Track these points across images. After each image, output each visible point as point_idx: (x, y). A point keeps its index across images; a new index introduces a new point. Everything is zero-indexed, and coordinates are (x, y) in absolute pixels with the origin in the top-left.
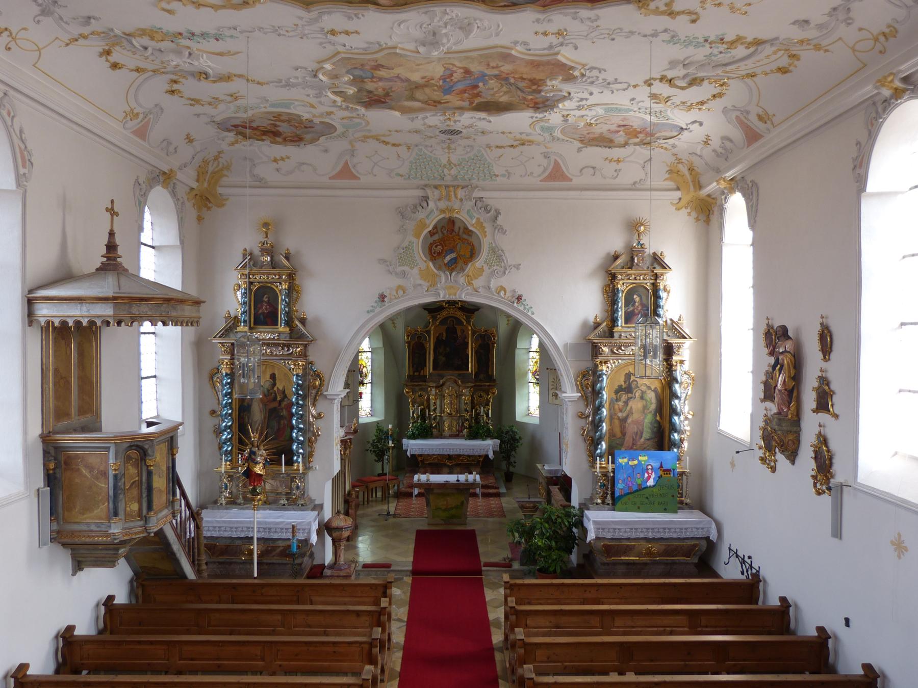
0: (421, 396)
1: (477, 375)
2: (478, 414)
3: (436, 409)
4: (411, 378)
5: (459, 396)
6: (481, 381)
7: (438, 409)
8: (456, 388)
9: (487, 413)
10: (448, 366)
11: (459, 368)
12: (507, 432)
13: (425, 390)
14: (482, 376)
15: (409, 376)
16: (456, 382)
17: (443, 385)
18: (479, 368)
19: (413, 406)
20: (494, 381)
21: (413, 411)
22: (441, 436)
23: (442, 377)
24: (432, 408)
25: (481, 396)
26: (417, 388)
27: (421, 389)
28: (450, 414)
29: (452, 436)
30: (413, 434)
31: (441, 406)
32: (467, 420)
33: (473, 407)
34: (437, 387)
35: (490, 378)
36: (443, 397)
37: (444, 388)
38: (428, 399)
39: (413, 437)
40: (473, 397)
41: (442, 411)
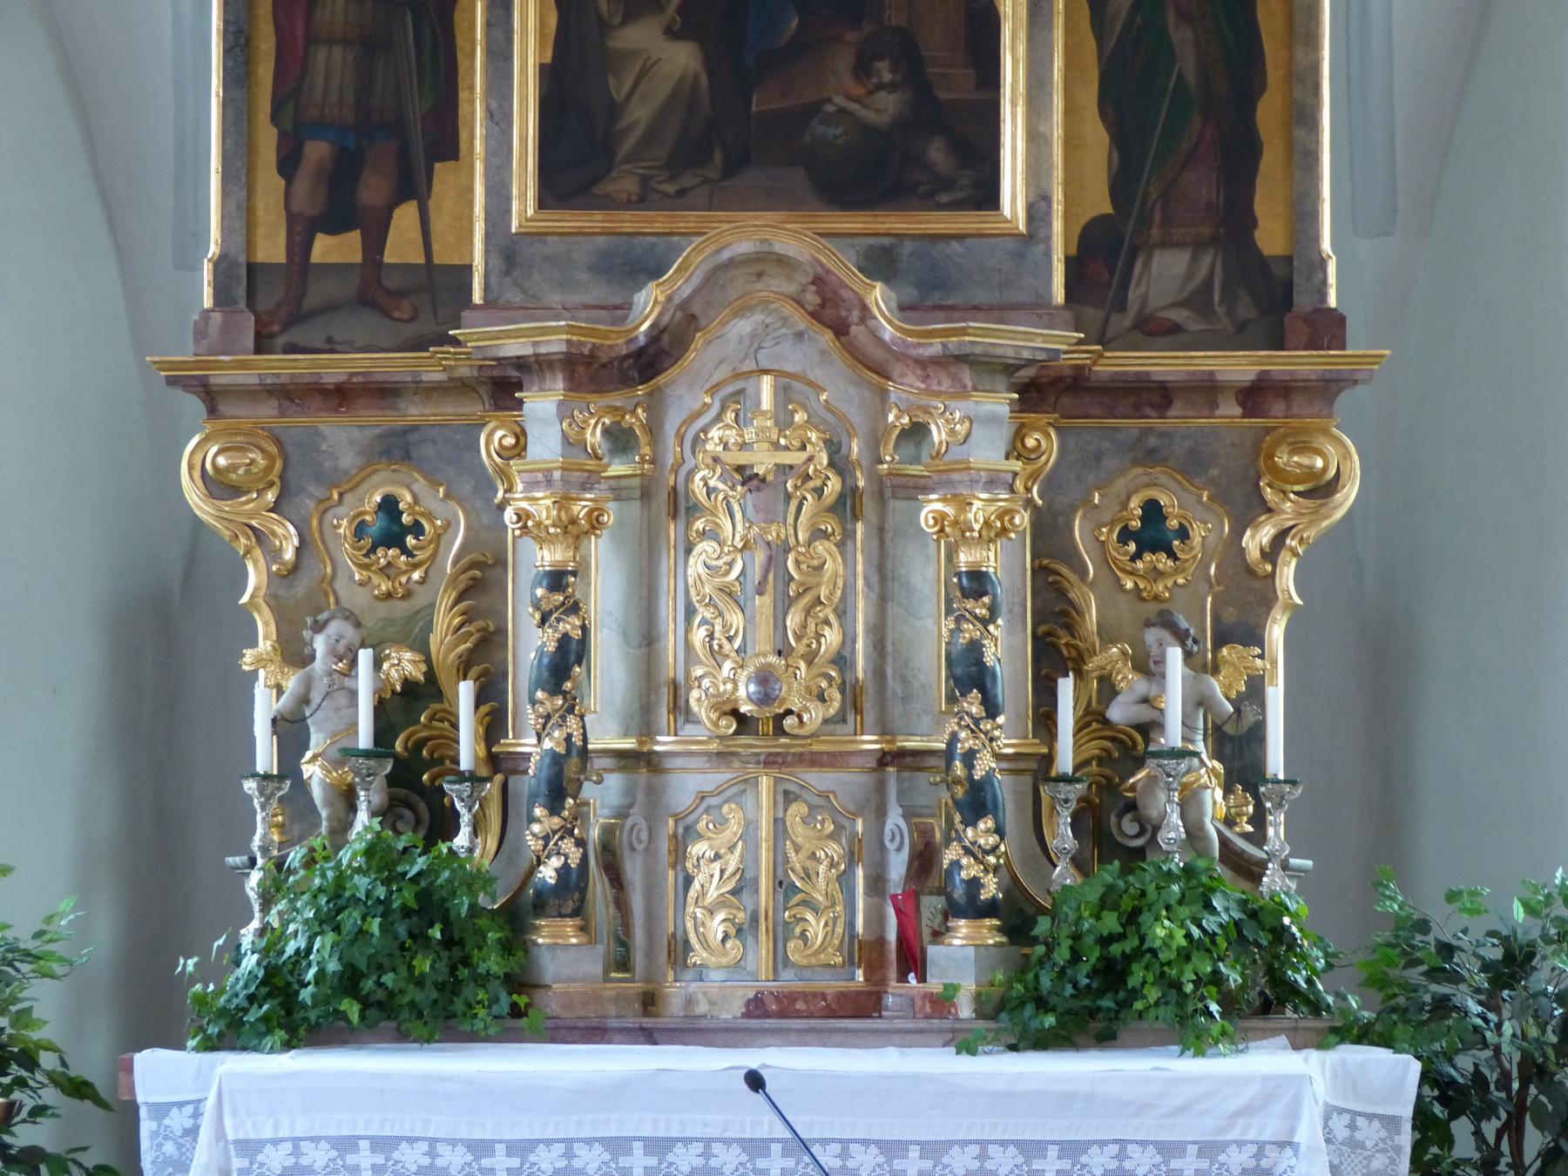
0: (393, 529)
1: (1101, 260)
2: (1124, 749)
3: (565, 662)
4: (272, 301)
5: (867, 502)
6: (1153, 331)
7: (608, 674)
8: (838, 388)
9: (1226, 711)
10: (725, 150)
11: (860, 177)
12: (1513, 964)
13: (454, 461)
14: (1166, 274)
15: (243, 280)
16: (832, 313)
17: (650, 362)
18: (1122, 184)
19: (294, 654)
20: (1327, 329)
21: (298, 708)
22: (648, 1020)
23: (642, 266)
24: (530, 644)
25: (1153, 534)
26: (341, 436)
27: (397, 449)
28: (756, 727)
29: (778, 1012)
30: (277, 982)
31: (647, 639)
32: (977, 802)
33: (1053, 653)
34: (587, 372)
35: (1271, 299)
36: (666, 506)
37: (686, 391)
38: (482, 579)
39: (285, 1012)
40: (1049, 538)
41: (658, 696)
